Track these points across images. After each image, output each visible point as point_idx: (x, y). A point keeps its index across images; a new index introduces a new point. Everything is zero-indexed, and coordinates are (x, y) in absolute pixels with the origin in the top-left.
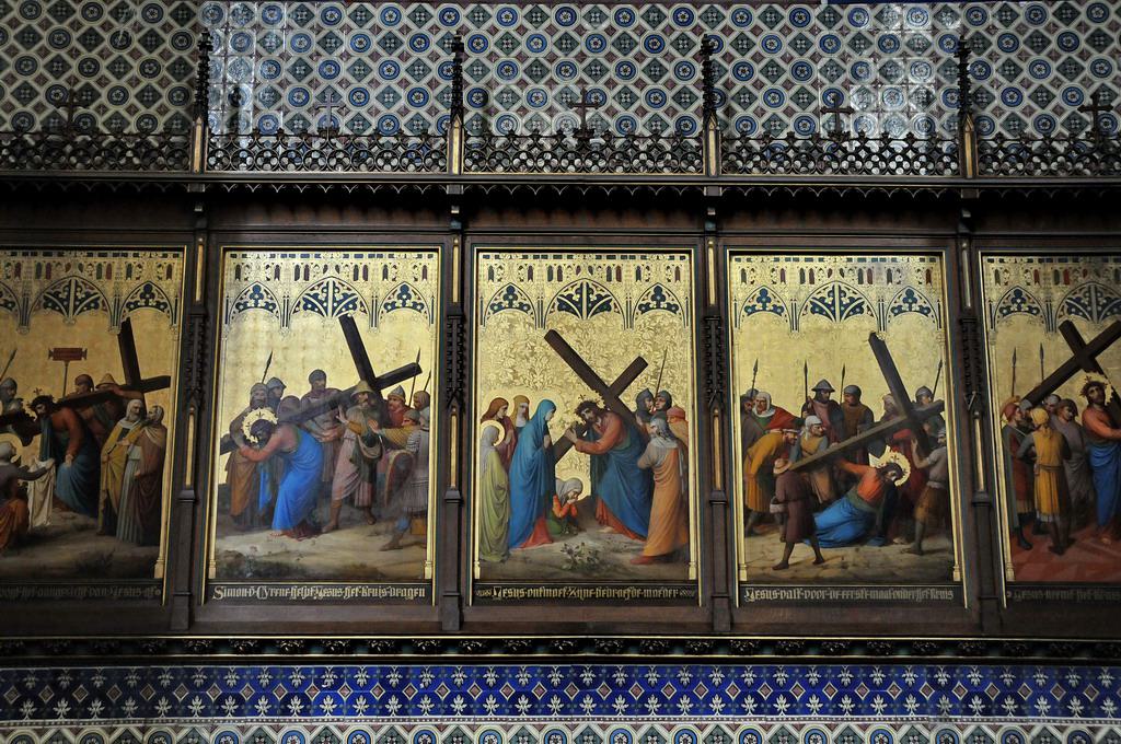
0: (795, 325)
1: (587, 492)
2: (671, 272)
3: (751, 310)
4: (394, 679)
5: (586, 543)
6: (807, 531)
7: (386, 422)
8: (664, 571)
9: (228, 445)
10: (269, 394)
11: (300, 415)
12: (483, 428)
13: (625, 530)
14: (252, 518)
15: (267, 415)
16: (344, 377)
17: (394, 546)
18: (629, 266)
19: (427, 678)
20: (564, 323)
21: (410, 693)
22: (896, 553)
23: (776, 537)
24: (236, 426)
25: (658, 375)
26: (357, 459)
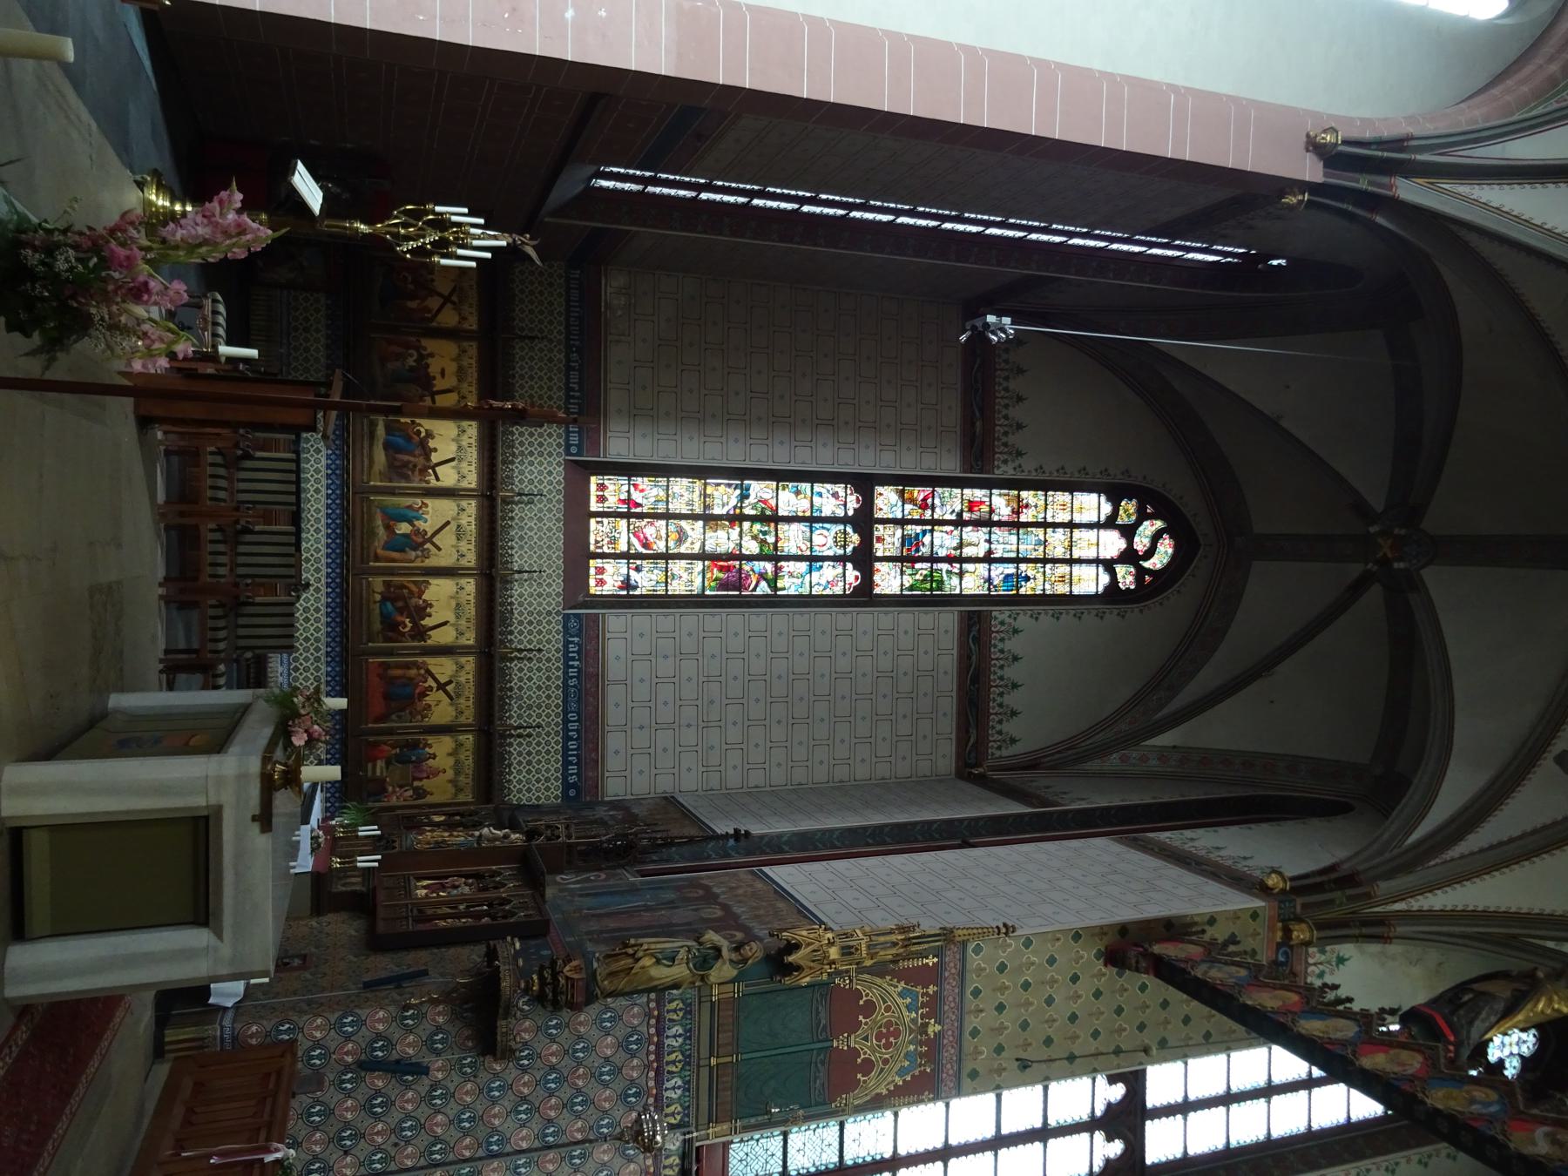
0: (452, 597)
1: (398, 532)
2: (470, 559)
3: (457, 584)
4: (338, 472)
5: (381, 531)
6: (385, 599)
7: (421, 471)
8: (372, 555)
10: (429, 435)
12: (419, 501)
13: (386, 543)
14: (389, 429)
15: (423, 434)
16: (435, 458)
17: (380, 473)
18: (472, 547)
19: (338, 482)
20: (453, 526)
21: (333, 477)
22: (377, 626)
24: (420, 425)
25: (436, 555)
26: (409, 462)
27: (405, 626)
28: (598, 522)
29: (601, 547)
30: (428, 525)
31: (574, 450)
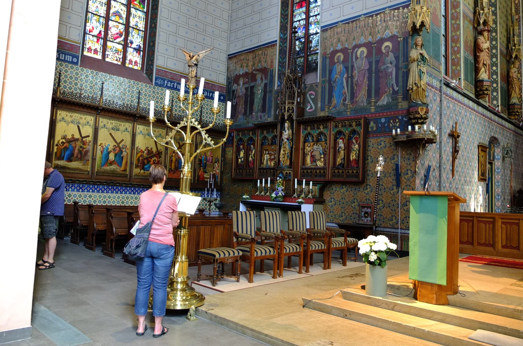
0: (145, 137)
1: (113, 159)
2: (128, 125)
3: (139, 134)
4: (81, 186)
5: (113, 167)
7: (84, 144)
8: (124, 172)
9: (57, 145)
10: (64, 137)
11: (69, 141)
12: (99, 147)
13: (118, 165)
14: (61, 158)
15: (64, 141)
16: (77, 136)
17: (84, 165)
18: (123, 124)
19: (86, 186)
20: (113, 132)
21: (83, 189)
23: (139, 169)
24: (58, 142)
25: (125, 142)
26: (79, 150)
27: (155, 160)
28: (107, 57)
29: (120, 59)
30: (111, 144)
31: (75, 60)
